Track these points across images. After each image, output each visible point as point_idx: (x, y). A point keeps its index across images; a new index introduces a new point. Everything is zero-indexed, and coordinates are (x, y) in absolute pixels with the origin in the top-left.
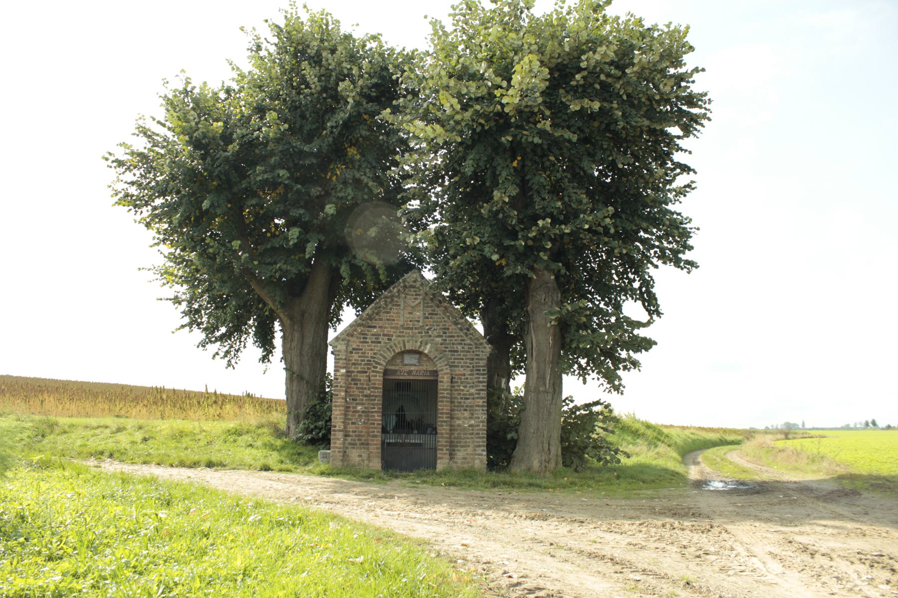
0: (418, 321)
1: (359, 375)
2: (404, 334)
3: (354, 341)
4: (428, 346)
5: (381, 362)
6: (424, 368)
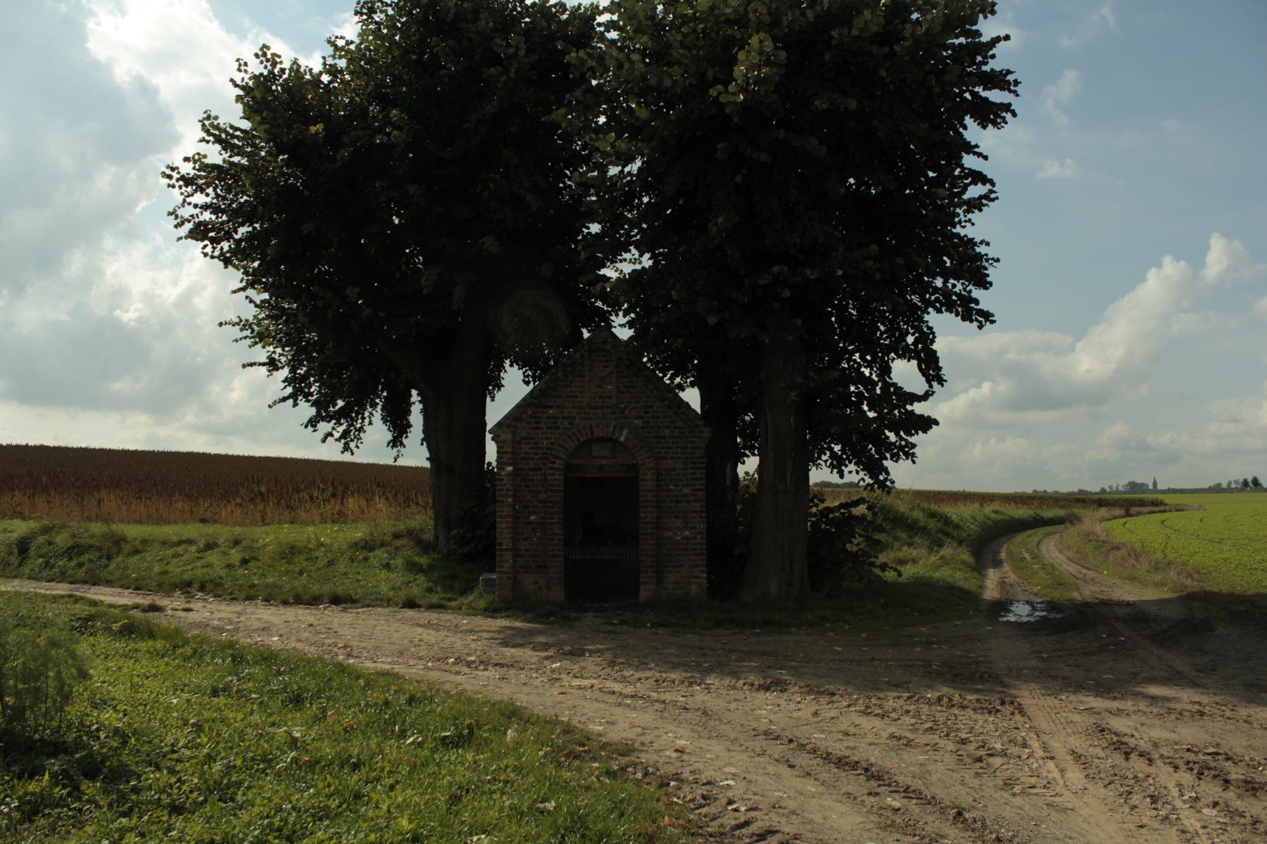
4: (625, 432)
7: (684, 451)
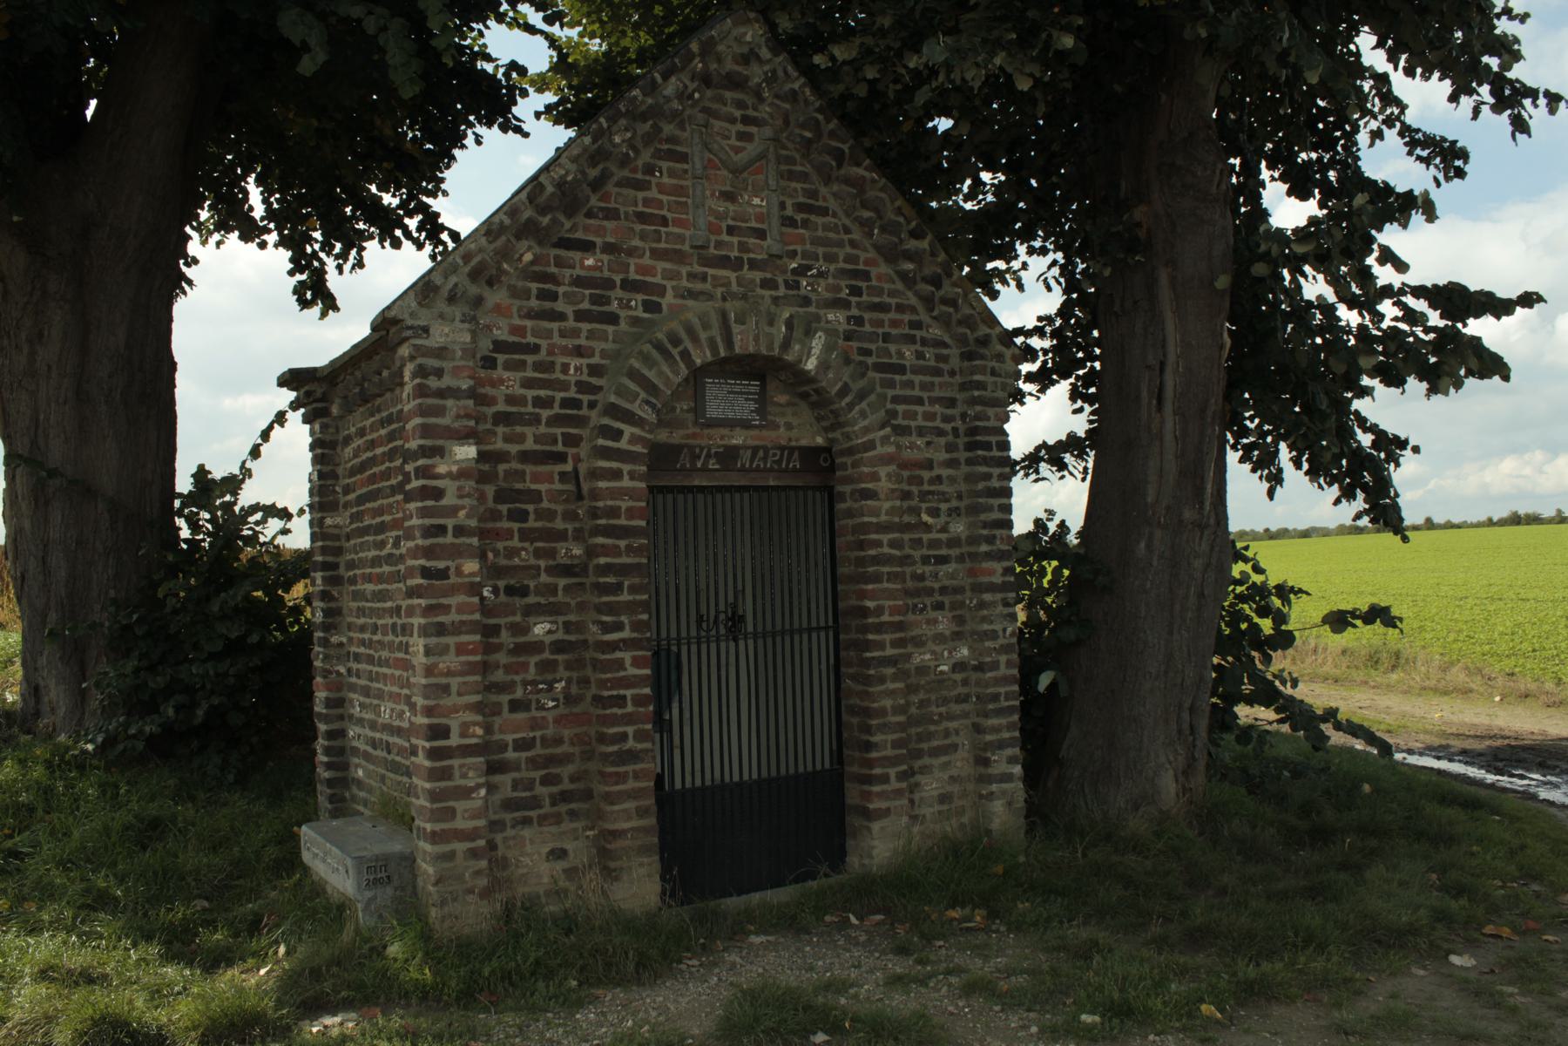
0: (761, 234)
1: (529, 469)
2: (708, 286)
4: (818, 343)
5: (635, 407)
6: (782, 436)
7: (949, 412)
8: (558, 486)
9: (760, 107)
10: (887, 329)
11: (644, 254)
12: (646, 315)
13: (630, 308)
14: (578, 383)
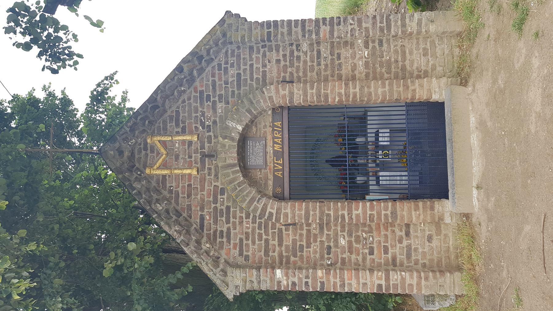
3: (228, 254)
4: (231, 124)
5: (260, 206)
8: (290, 232)
9: (139, 142)
10: (223, 82)
11: (202, 194)
12: (226, 194)
13: (224, 201)
14: (253, 223)
